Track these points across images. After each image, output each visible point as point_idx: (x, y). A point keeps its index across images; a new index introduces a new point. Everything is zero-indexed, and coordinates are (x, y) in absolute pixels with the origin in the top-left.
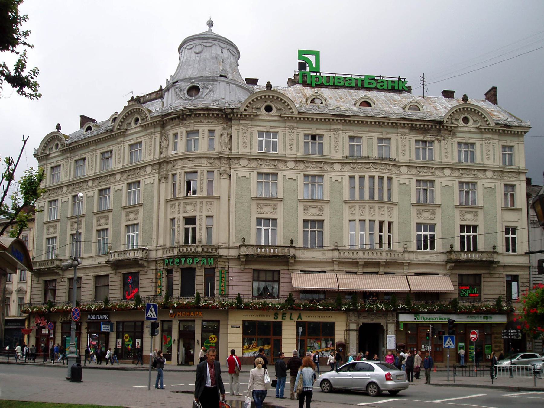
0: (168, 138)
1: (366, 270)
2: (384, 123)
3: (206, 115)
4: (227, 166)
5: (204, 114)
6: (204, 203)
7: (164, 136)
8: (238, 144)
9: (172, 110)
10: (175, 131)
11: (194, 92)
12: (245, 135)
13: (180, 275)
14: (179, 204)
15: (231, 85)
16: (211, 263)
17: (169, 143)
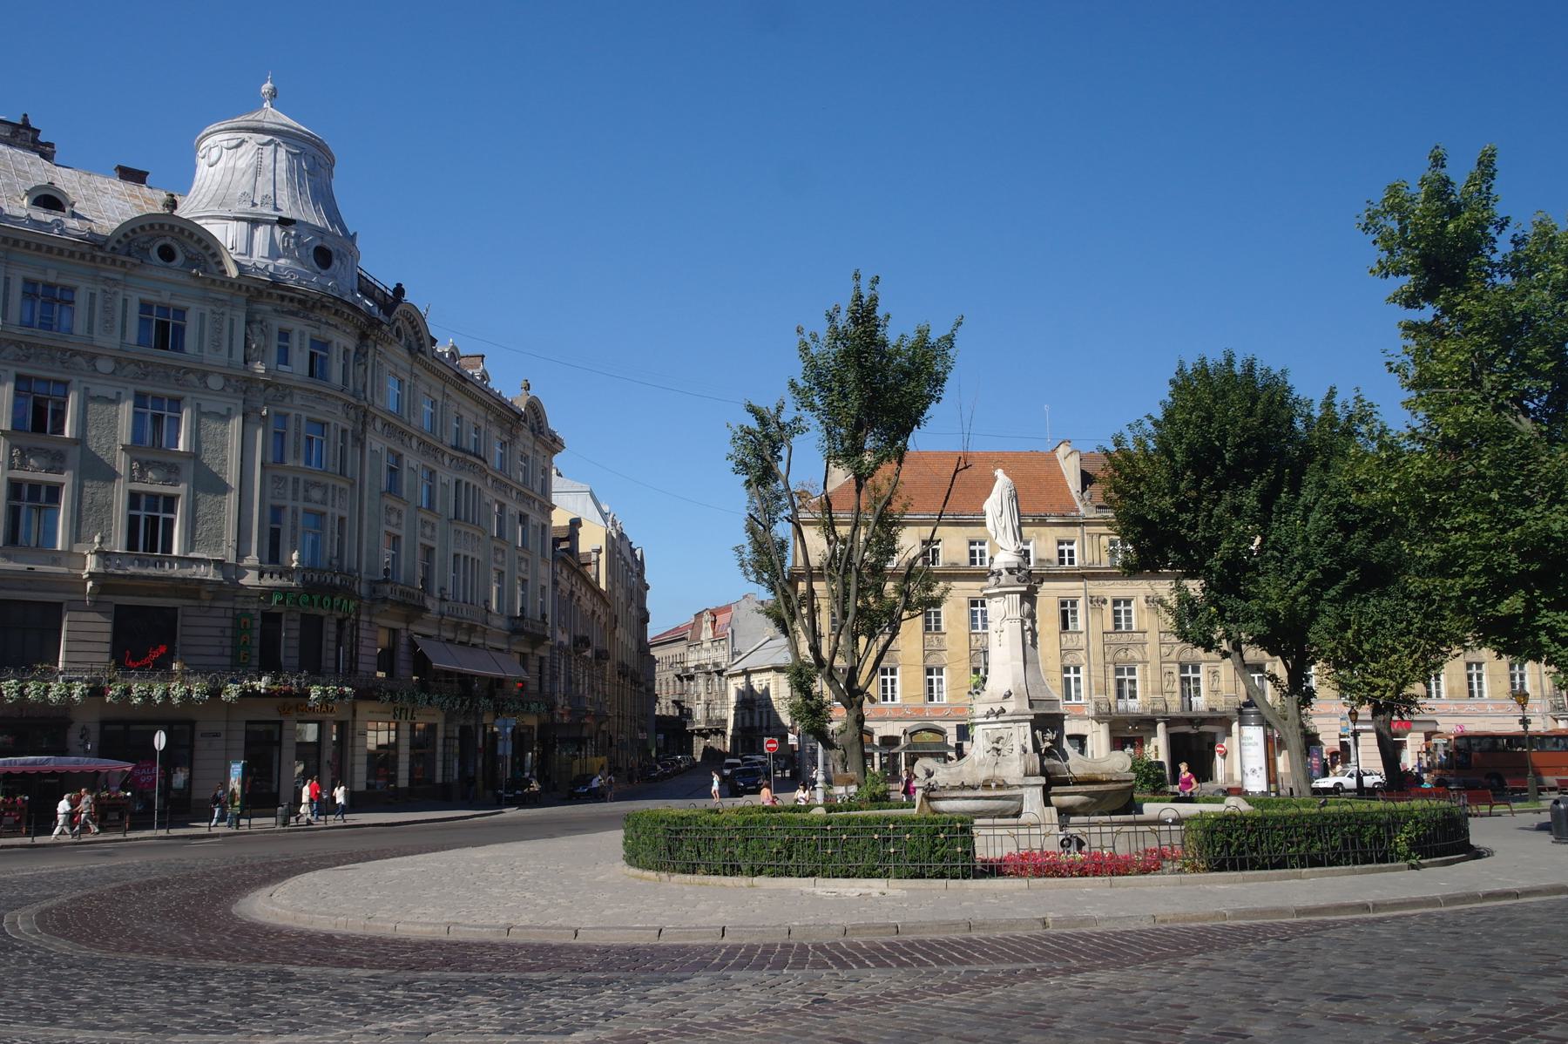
5: (349, 315)
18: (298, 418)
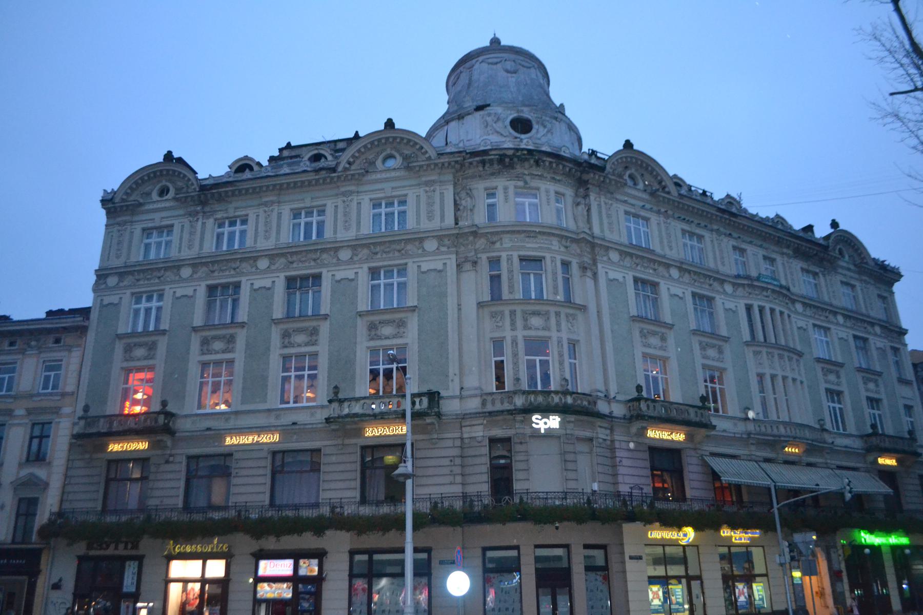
3: (554, 165)
6: (563, 316)
7: (462, 191)
8: (601, 224)
9: (489, 147)
14: (513, 313)
18: (509, 259)
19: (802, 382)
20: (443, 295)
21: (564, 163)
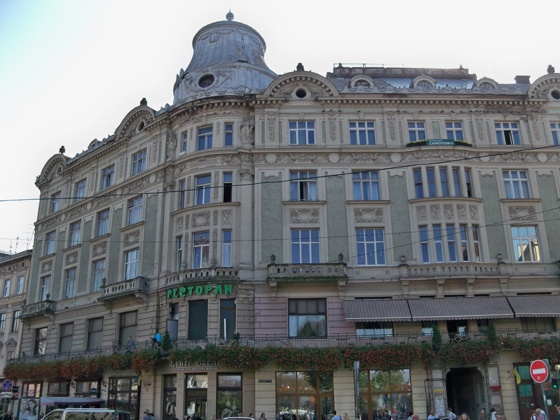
0: (176, 139)
1: (448, 292)
2: (451, 102)
3: (222, 104)
4: (250, 164)
6: (219, 213)
9: (180, 104)
10: (183, 129)
11: (208, 81)
12: (272, 126)
13: (188, 311)
14: (188, 217)
15: (253, 71)
16: (228, 292)
17: (176, 144)
19: (476, 226)
20: (156, 212)
21: (228, 101)
